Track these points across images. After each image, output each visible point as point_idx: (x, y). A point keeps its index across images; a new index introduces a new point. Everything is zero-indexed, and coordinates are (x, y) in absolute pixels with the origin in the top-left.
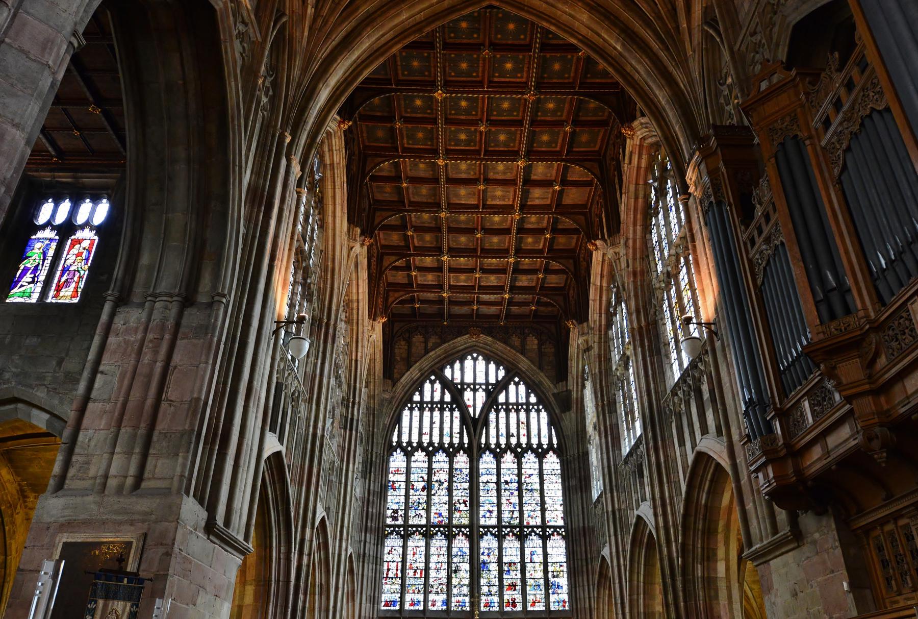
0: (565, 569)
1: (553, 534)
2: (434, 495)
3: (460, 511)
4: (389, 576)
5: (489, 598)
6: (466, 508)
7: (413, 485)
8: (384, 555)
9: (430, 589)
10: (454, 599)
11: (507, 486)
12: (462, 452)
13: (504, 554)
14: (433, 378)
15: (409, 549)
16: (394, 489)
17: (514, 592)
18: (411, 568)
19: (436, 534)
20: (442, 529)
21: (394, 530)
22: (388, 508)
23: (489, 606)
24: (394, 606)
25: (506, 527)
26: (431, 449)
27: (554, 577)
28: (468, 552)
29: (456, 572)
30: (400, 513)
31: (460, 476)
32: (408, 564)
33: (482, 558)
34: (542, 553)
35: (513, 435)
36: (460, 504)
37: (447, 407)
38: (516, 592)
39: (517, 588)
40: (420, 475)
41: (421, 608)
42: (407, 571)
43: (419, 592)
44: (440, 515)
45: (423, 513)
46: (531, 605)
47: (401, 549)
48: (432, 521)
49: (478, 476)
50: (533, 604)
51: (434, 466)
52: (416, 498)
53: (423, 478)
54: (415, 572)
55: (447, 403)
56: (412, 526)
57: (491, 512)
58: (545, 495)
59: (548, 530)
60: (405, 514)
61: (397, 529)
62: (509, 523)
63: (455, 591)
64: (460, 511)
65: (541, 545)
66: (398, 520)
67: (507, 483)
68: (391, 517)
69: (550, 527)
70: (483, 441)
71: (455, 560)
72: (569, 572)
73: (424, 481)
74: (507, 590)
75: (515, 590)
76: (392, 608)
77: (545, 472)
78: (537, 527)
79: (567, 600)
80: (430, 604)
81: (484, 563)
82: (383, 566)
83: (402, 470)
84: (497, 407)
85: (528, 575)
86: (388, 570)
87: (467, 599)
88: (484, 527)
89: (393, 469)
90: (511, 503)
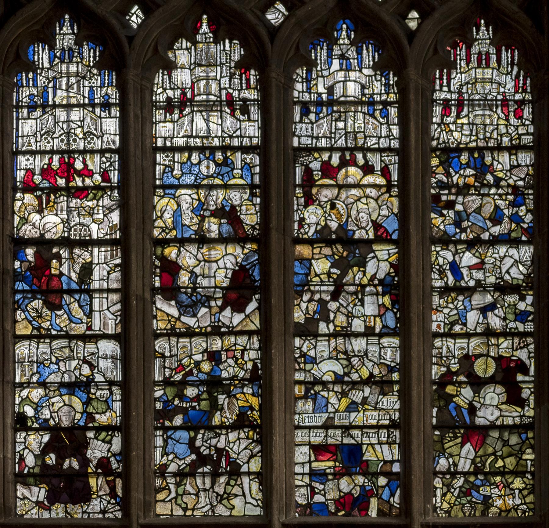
31: (473, 201)
40: (218, 196)
89: (39, 163)
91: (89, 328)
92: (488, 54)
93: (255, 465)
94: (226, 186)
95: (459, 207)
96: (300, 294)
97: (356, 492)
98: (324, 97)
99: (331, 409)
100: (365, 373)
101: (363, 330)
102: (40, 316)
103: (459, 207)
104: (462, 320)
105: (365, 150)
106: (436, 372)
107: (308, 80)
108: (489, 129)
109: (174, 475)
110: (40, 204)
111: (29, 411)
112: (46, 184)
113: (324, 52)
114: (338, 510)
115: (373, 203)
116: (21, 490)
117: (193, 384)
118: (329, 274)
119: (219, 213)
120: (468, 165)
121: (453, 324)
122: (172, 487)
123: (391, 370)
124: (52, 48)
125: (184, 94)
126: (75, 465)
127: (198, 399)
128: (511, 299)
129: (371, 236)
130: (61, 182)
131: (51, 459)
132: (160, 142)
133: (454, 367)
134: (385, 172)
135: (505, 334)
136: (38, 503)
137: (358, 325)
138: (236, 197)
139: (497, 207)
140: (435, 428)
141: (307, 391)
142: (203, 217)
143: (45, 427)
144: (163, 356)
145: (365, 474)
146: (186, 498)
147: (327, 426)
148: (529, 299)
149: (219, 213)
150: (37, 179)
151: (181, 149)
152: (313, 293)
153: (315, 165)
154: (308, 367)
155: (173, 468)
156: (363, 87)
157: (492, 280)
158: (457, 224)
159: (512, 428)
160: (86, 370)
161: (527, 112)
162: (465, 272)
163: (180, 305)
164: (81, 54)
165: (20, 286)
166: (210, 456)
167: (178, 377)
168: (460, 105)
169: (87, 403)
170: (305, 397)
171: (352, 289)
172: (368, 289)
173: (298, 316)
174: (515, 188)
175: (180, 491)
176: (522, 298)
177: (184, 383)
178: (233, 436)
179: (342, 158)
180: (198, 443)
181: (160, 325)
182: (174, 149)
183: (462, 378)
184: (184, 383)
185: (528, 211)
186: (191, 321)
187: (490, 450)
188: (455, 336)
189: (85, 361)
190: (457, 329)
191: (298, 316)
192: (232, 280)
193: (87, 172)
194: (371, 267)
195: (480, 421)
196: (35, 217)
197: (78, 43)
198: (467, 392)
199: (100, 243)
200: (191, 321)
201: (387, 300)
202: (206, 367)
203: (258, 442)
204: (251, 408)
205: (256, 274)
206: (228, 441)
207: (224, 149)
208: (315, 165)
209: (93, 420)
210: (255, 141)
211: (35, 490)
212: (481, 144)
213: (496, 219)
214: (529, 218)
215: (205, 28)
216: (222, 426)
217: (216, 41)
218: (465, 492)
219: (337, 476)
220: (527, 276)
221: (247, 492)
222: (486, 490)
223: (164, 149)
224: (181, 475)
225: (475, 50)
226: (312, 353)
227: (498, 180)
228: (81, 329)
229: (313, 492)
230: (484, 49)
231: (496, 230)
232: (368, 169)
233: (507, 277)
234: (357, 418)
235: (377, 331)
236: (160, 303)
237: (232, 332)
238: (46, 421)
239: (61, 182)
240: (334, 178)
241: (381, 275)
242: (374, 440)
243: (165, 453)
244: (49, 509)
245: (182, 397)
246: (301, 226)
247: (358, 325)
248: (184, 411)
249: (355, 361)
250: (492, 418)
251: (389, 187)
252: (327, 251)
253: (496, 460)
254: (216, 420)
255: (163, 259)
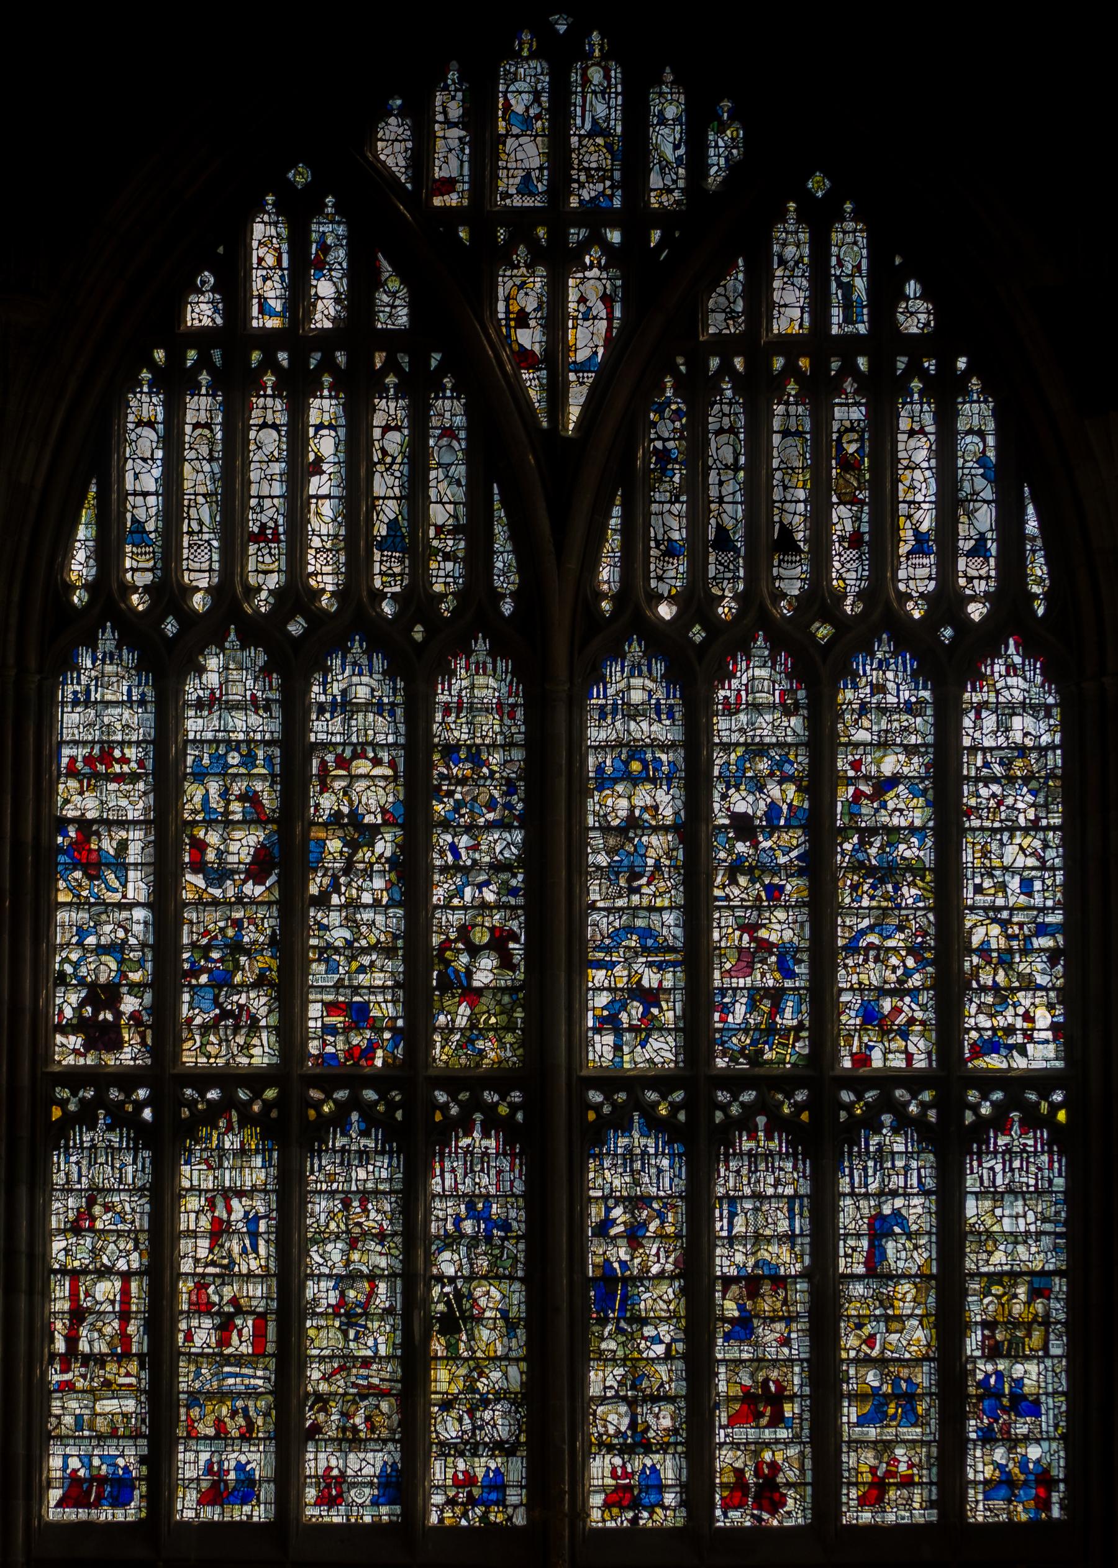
0: (1058, 1310)
1: (999, 1122)
2: (322, 902)
3: (472, 995)
4: (84, 1346)
5: (637, 1463)
6: (507, 979)
7: (200, 846)
8: (47, 1236)
9: (310, 1417)
10: (439, 1471)
11: (741, 847)
12: (481, 646)
13: (720, 1226)
14: (300, 176)
15: (193, 1203)
16: (93, 868)
17: (768, 1434)
18: (202, 1308)
19: (339, 1120)
20: (370, 1095)
21: (101, 1100)
22: (62, 978)
23: (636, 1505)
24: (120, 1501)
25: (734, 1082)
26: (295, 628)
27: (993, 1352)
28: (516, 1216)
29: (450, 1325)
30: (129, 1004)
32: (185, 1286)
33: (597, 1252)
34: (927, 1223)
35: (786, 543)
36: (474, 951)
37: (391, 365)
38: (783, 1434)
39: (788, 1410)
41: (259, 1513)
42: (183, 1326)
43: (247, 1436)
44: (359, 1015)
45: (259, 1003)
46: (862, 1501)
47: (144, 1205)
48: (313, 1047)
49: (578, 792)
50: (875, 1493)
51: (322, 729)
52: (214, 920)
53: (250, 798)
54: (225, 1327)
55: (391, 340)
56: (203, 1079)
57: (650, 997)
58: (968, 893)
59: (973, 1096)
60: (155, 1009)
61: (114, 1094)
62: (755, 1058)
63: (449, 1429)
64: (472, 995)
65: (930, 1183)
66: (117, 1045)
67: (743, 826)
68: (79, 1026)
69: (988, 1082)
70: (607, 574)
71: (447, 1263)
72: (1075, 1330)
73: (256, 817)
74: (732, 1421)
75: (777, 1420)
76: (106, 1514)
77: (972, 765)
78: (913, 1081)
79: (1058, 1472)
80: (311, 1494)
81: (608, 1277)
82: (46, 1295)
83: (131, 753)
84: (697, 363)
85: (850, 1342)
86: (77, 1315)
87: (516, 1470)
88: (610, 1081)
89: (81, 752)
90: (765, 946)
91: (124, 897)
92: (484, 663)
93: (273, 1020)
94: (249, 775)
95: (458, 796)
96: (315, 870)
97: (364, 1044)
98: (339, 699)
99: (341, 970)
100: (373, 941)
101: (370, 901)
102: (80, 885)
103: (458, 796)
104: (460, 893)
105: (374, 745)
106: (436, 940)
107: (325, 683)
108: (485, 728)
109: (200, 1026)
110: (82, 787)
111: (68, 969)
112: (87, 770)
113: (339, 662)
114: (347, 1060)
115: (381, 792)
116: (59, 1038)
117: (217, 947)
118: (341, 852)
119: (241, 798)
120: (466, 760)
121: (452, 897)
122: (197, 1037)
123: (395, 937)
124: (95, 650)
125: (213, 693)
126: (110, 1017)
127: (221, 960)
128: (504, 876)
129: (380, 821)
130: (102, 768)
131: (88, 1011)
132: (191, 736)
133: (453, 936)
134: (392, 764)
135: (499, 906)
136: (75, 1051)
137: (367, 898)
138: (259, 786)
139: (492, 796)
140: (436, 988)
141: (321, 954)
142: (228, 802)
143: (82, 982)
144: (191, 923)
145: (372, 1028)
146: (209, 1048)
147: (338, 986)
148: (520, 877)
149: (241, 798)
150: (79, 765)
151: (209, 742)
152: (327, 869)
153: (330, 758)
154: (322, 933)
155: (198, 1021)
156: (373, 690)
157: (487, 859)
158: (456, 809)
159: (504, 990)
160: (121, 934)
161: (519, 714)
162: (463, 852)
163: (206, 878)
164: (120, 657)
165: (62, 859)
166: (232, 1011)
167: (204, 941)
168: (459, 709)
169: (121, 962)
170: (319, 960)
171: (361, 866)
172: (376, 867)
173: (314, 890)
174: (509, 781)
175: (205, 1041)
176: (514, 876)
177: (208, 948)
178: (252, 995)
179: (354, 752)
180: (221, 999)
181: (188, 895)
182: (202, 742)
183: (460, 946)
184: (208, 948)
185: (520, 800)
186: (217, 892)
187: (485, 1008)
188: (454, 908)
189: (120, 926)
190: (456, 902)
191: (314, 890)
192: (254, 856)
193: (124, 760)
194: (379, 847)
195: (476, 984)
196: (76, 798)
197: (119, 647)
198: (464, 959)
199: (135, 823)
200: (217, 892)
201: (393, 876)
202: (230, 932)
203: (276, 999)
204: (271, 970)
205: (276, 852)
206: (248, 998)
207: (248, 742)
208: (330, 758)
209: (127, 977)
210: (276, 735)
211: (72, 1038)
212: (478, 741)
213: (491, 805)
214: (520, 806)
215: (232, 636)
216: (242, 984)
217: (242, 648)
218: (460, 1046)
219: (346, 1030)
220: (518, 857)
221: (265, 1043)
222: (480, 1044)
223: (194, 741)
224: (205, 1029)
225: (473, 659)
226: (325, 921)
227: (492, 772)
228: (116, 897)
229: (325, 1044)
230: (481, 659)
231: (490, 816)
232: (377, 762)
233: (500, 857)
234: (363, 979)
235: (384, 901)
236: (189, 877)
237: (254, 902)
238: (84, 977)
239: (102, 768)
240: (348, 769)
241: (388, 854)
242: (380, 998)
243: (191, 1008)
244: (84, 1055)
245: (208, 959)
246: (316, 810)
247: (367, 898)
248: (210, 971)
249: (364, 929)
250: (486, 981)
251: (395, 777)
252: (340, 833)
253: (489, 1018)
254: (238, 978)
255: (192, 837)
